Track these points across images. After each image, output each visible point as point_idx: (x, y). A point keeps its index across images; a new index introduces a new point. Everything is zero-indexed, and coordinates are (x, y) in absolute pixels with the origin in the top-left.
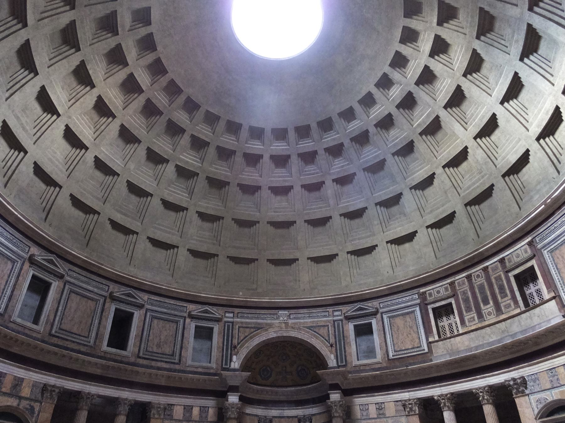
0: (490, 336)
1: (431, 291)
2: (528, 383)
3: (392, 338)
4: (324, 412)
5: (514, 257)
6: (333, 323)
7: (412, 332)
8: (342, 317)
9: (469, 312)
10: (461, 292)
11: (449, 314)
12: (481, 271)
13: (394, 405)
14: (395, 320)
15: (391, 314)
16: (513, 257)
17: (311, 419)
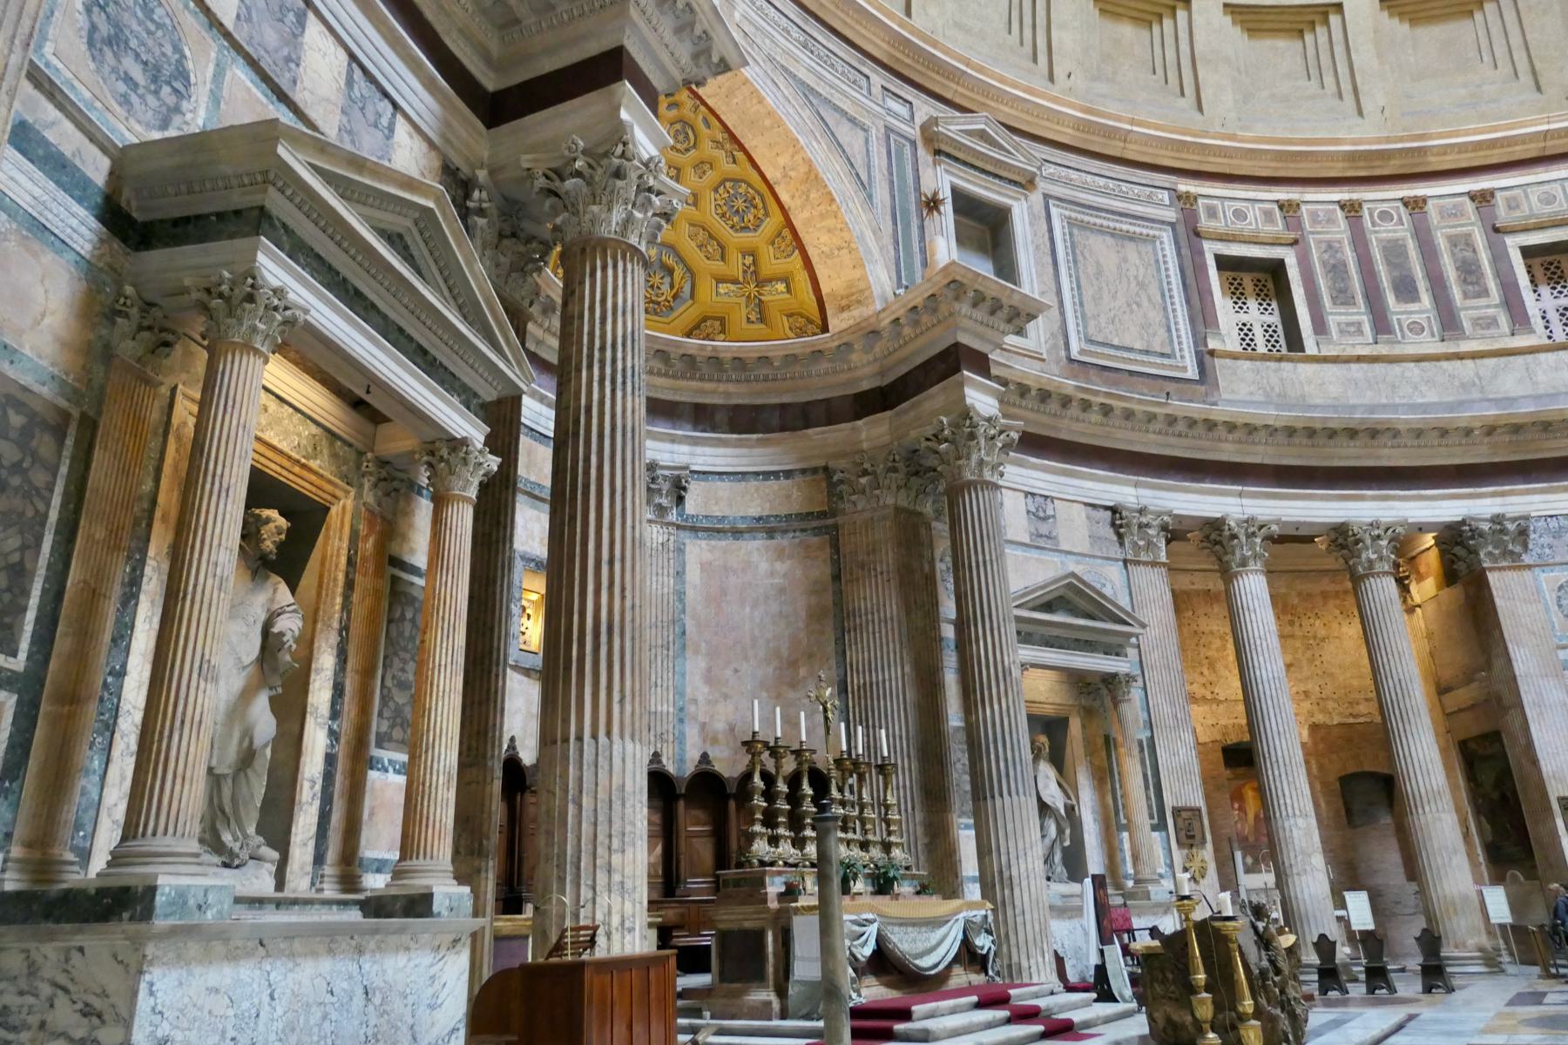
0: (1416, 388)
1: (1215, 202)
2: (1532, 536)
3: (1080, 295)
4: (767, 475)
5: (1534, 199)
6: (883, 130)
7: (1145, 303)
8: (912, 131)
9: (1342, 304)
10: (1319, 242)
11: (1242, 294)
12: (1399, 204)
13: (1084, 516)
14: (1087, 239)
15: (1080, 217)
16: (1527, 196)
17: (684, 489)
